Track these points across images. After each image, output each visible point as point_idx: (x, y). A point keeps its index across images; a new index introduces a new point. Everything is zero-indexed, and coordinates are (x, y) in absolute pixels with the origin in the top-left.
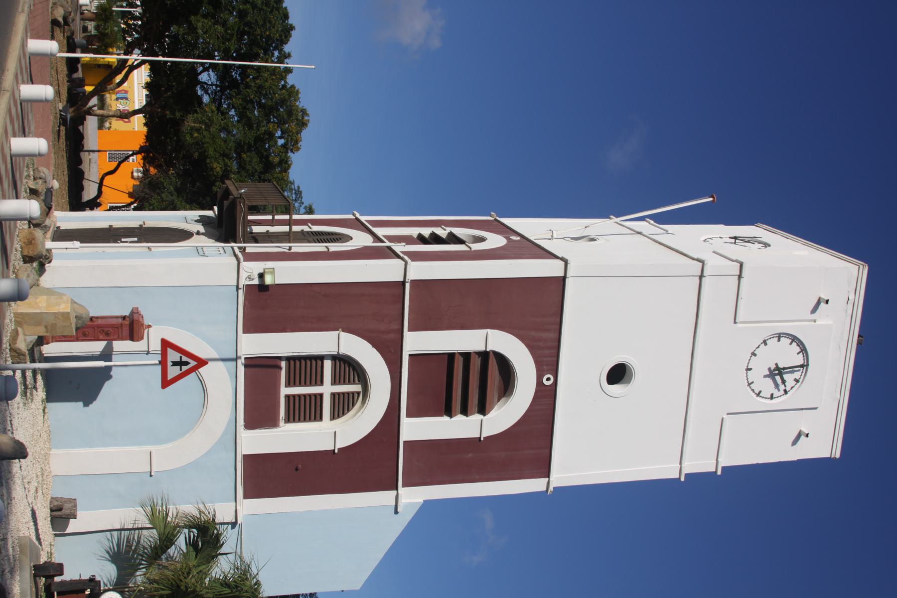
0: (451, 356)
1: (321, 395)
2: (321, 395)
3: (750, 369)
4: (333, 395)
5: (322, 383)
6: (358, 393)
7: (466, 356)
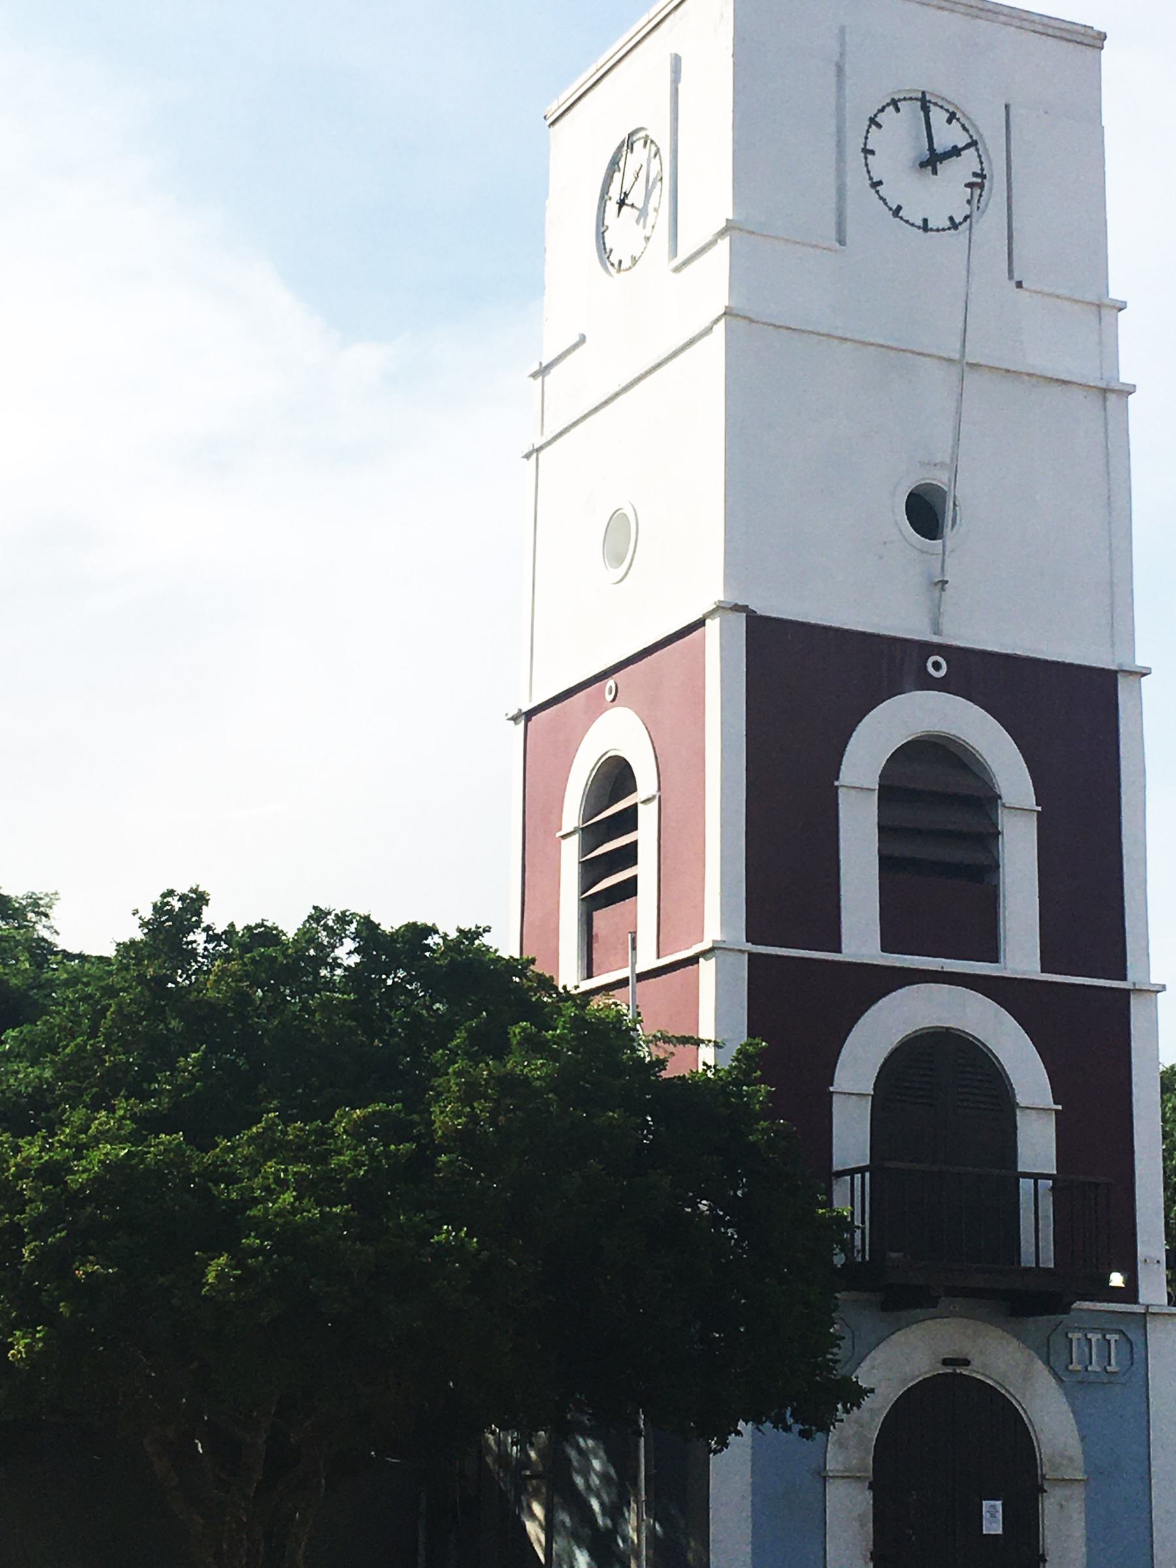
0: (887, 863)
3: (925, 221)
7: (884, 830)
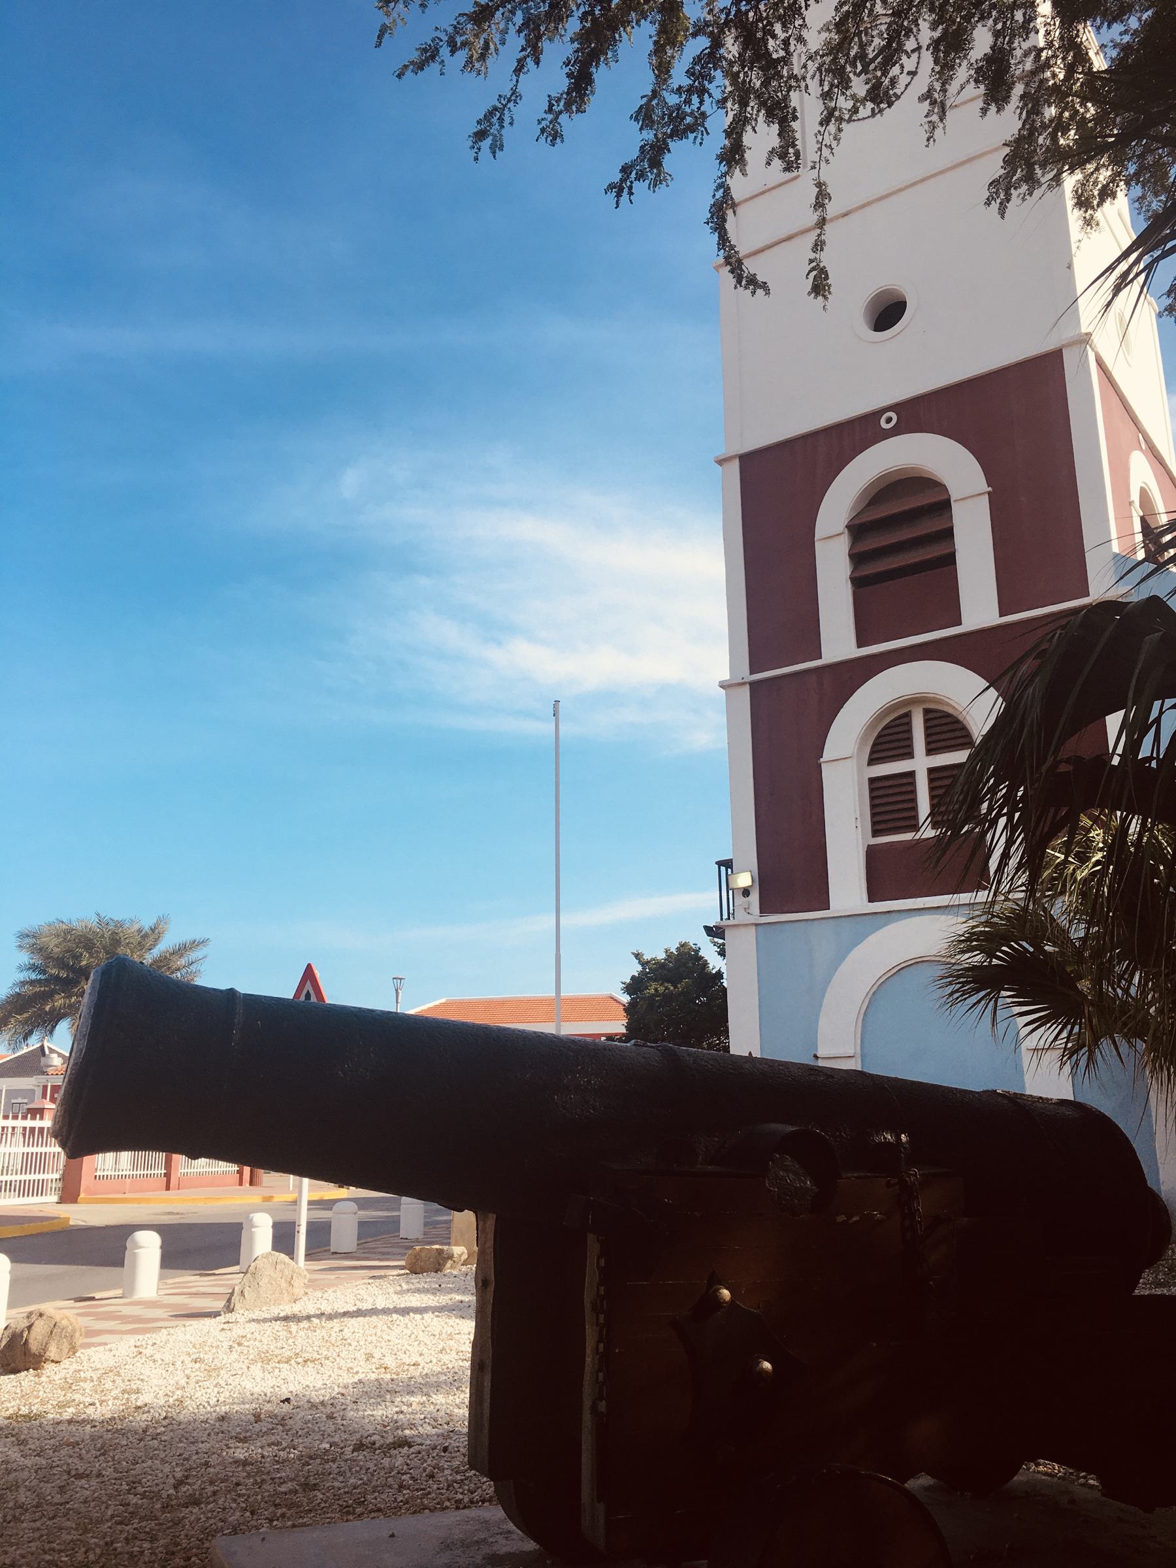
1: (931, 771)
2: (931, 771)
4: (930, 751)
5: (912, 774)
6: (927, 712)
